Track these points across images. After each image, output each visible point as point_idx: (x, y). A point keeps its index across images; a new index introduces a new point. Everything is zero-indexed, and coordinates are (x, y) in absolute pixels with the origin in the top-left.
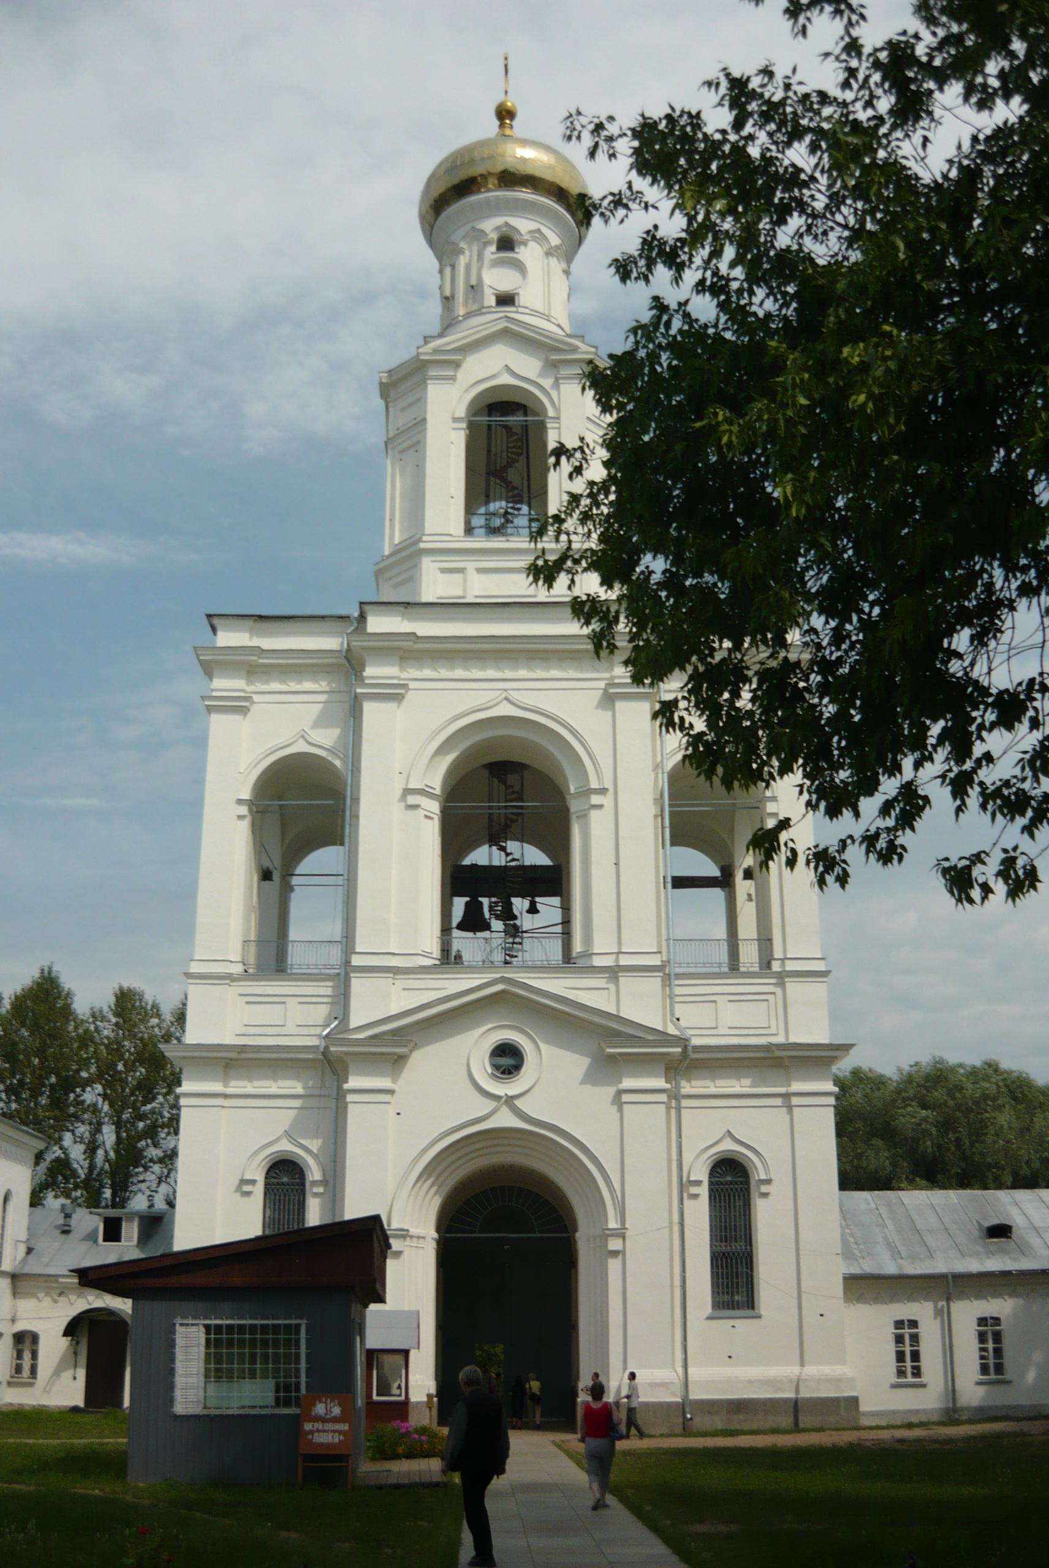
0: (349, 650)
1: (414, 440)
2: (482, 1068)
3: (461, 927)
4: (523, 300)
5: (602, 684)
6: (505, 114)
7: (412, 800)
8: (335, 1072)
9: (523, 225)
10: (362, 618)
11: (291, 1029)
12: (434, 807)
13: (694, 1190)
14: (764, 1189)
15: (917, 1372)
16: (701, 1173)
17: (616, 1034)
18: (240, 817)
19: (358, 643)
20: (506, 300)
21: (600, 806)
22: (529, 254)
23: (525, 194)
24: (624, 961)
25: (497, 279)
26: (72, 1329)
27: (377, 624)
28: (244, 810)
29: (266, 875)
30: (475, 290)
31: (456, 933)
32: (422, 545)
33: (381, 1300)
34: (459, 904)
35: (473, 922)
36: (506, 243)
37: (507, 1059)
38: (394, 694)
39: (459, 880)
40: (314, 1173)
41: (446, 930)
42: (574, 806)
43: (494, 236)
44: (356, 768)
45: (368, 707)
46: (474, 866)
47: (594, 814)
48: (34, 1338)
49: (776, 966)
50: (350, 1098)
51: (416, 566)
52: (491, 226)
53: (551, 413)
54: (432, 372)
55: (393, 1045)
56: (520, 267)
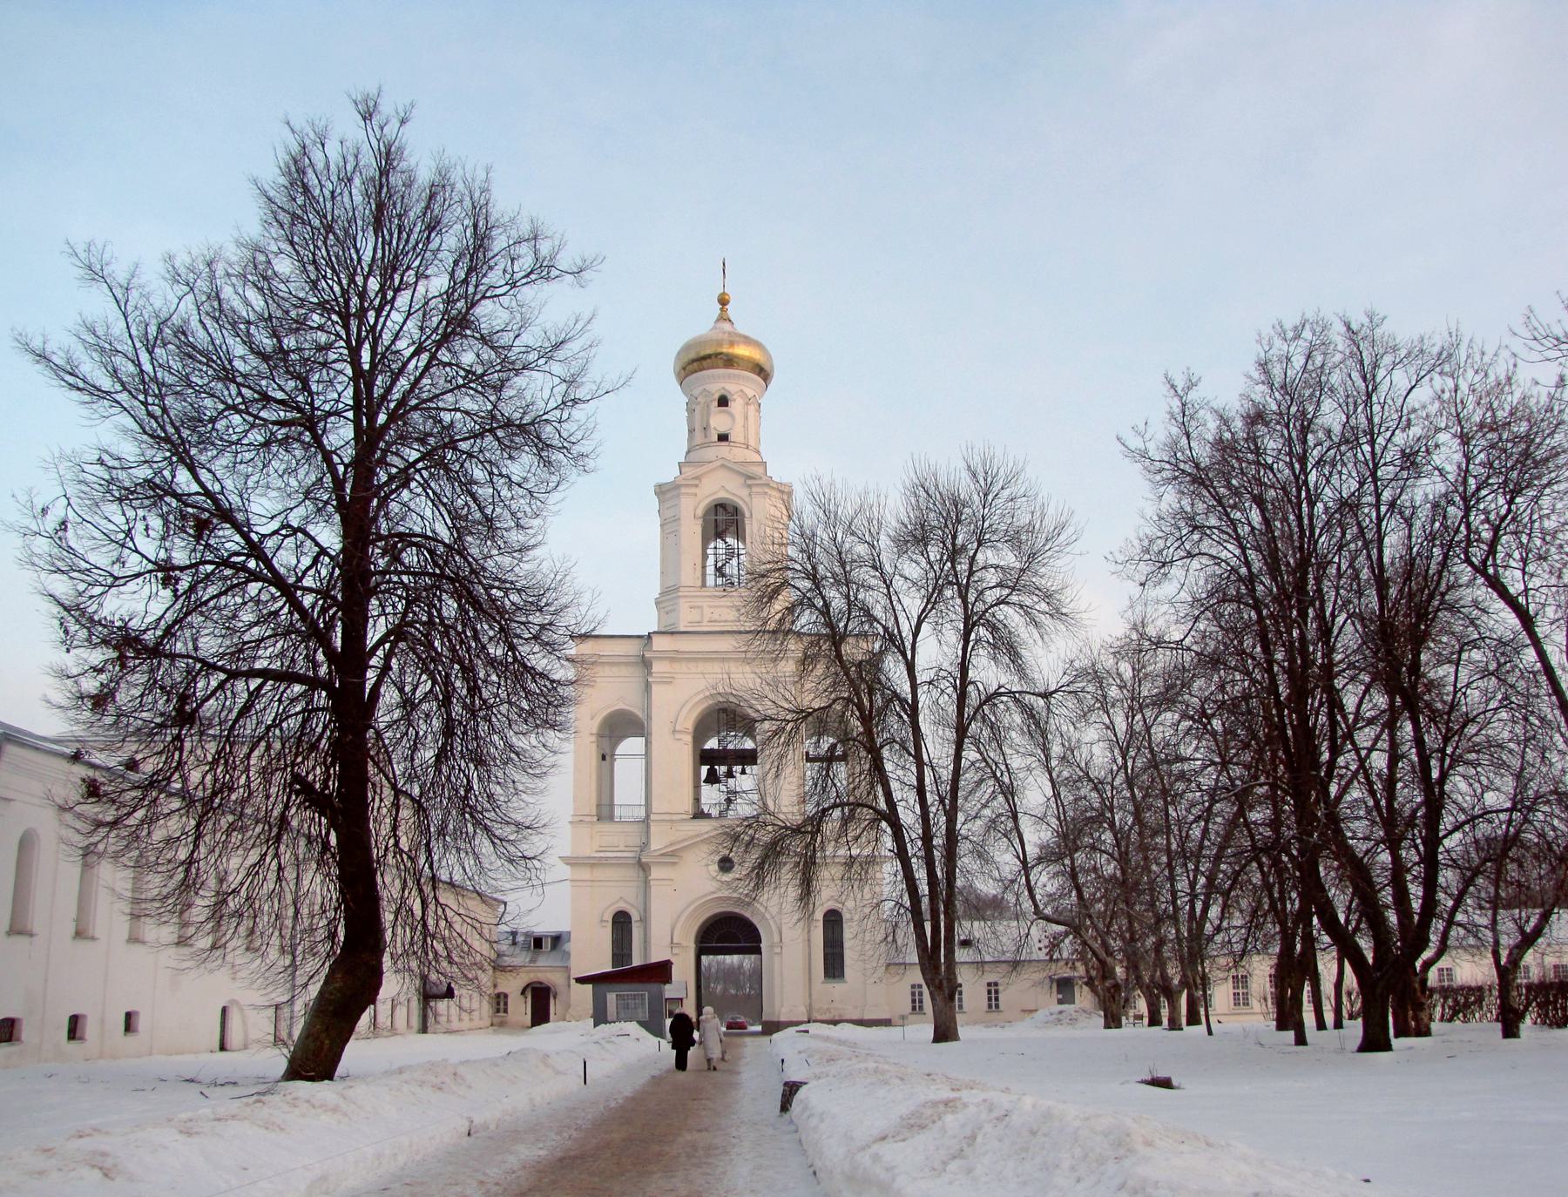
4: (731, 438)
6: (723, 301)
7: (678, 736)
9: (731, 388)
15: (997, 1006)
20: (723, 438)
26: (523, 993)
27: (660, 643)
28: (593, 739)
29: (604, 758)
34: (704, 769)
35: (713, 778)
36: (723, 402)
38: (668, 681)
40: (635, 917)
41: (697, 787)
43: (717, 396)
44: (649, 717)
45: (655, 688)
48: (506, 996)
52: (716, 389)
53: (747, 514)
54: (683, 490)
55: (672, 856)
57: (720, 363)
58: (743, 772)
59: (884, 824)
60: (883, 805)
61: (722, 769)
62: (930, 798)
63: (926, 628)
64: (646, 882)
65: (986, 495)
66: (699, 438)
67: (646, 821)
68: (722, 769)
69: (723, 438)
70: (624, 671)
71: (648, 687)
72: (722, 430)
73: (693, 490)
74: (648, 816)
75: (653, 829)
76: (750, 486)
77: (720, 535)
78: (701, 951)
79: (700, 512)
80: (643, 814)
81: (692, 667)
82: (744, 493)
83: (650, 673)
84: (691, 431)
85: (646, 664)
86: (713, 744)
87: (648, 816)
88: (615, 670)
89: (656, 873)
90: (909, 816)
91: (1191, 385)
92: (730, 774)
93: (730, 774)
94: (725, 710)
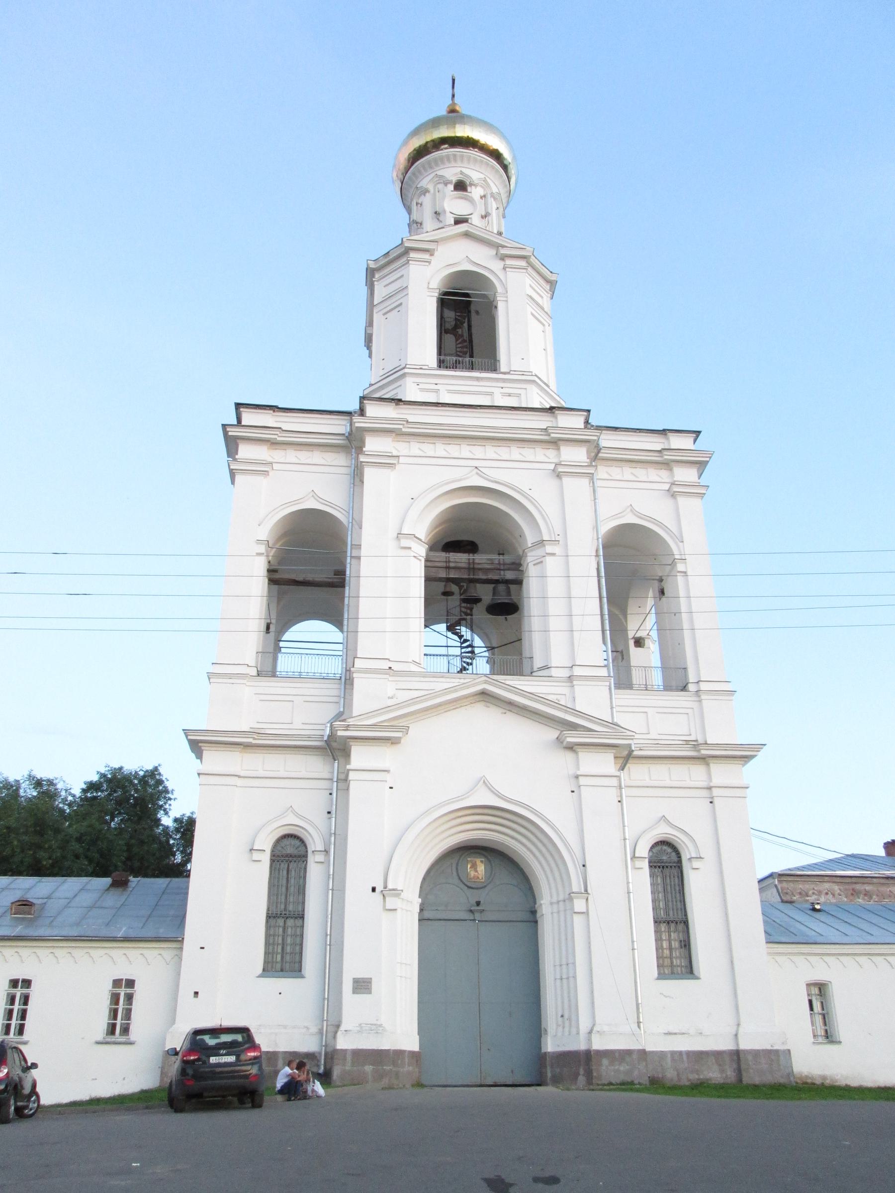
0: (350, 434)
1: (399, 302)
5: (552, 467)
7: (405, 542)
10: (362, 412)
12: (422, 550)
13: (638, 864)
14: (696, 864)
16: (643, 851)
17: (574, 727)
18: (259, 554)
19: (359, 422)
21: (553, 554)
23: (474, 153)
24: (577, 671)
25: (454, 205)
28: (262, 549)
32: (406, 370)
38: (388, 462)
40: (315, 843)
42: (531, 558)
43: (454, 179)
45: (368, 472)
47: (548, 559)
49: (692, 687)
50: (352, 775)
52: (452, 173)
53: (500, 289)
54: (412, 255)
64: (344, 781)
67: (347, 681)
70: (317, 457)
71: (357, 476)
73: (426, 256)
76: (503, 258)
81: (428, 448)
82: (497, 266)
85: (353, 443)
87: (348, 671)
88: (304, 456)
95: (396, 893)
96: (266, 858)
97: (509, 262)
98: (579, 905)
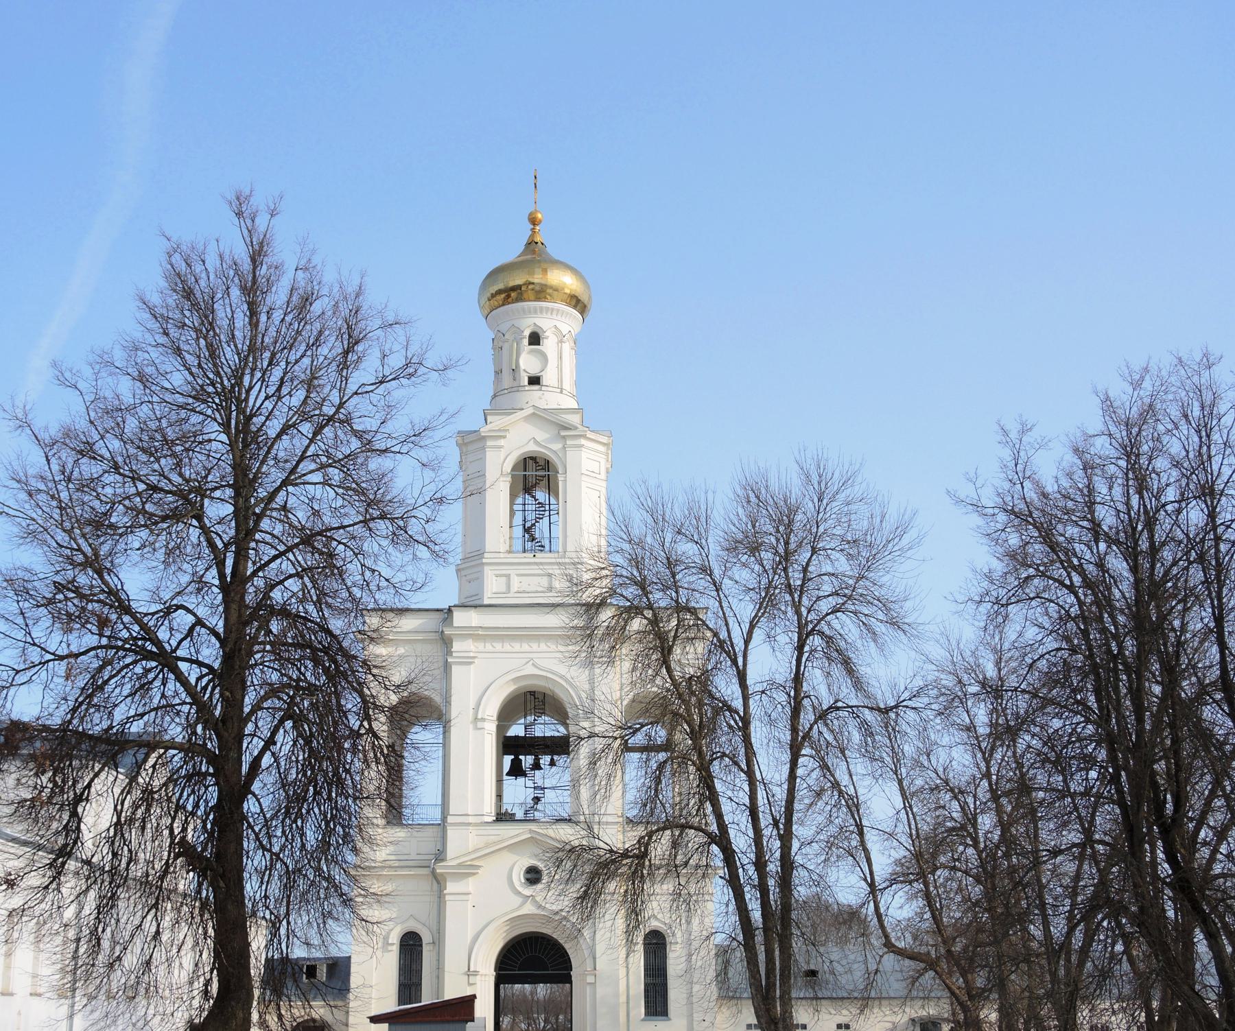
2: (519, 877)
3: (508, 774)
4: (544, 381)
6: (534, 221)
8: (438, 882)
11: (413, 856)
20: (535, 381)
22: (549, 344)
27: (460, 618)
30: (515, 371)
31: (505, 777)
33: (473, 1020)
34: (508, 759)
35: (516, 771)
36: (535, 339)
37: (533, 876)
38: (468, 662)
39: (509, 745)
40: (426, 939)
41: (499, 781)
43: (527, 333)
44: (448, 701)
45: (454, 668)
46: (517, 737)
50: (447, 898)
51: (482, 572)
54: (489, 443)
56: (544, 358)
57: (531, 294)
58: (552, 763)
59: (715, 848)
60: (714, 828)
61: (527, 761)
62: (765, 820)
63: (758, 635)
64: (441, 897)
65: (820, 500)
66: (507, 381)
68: (527, 761)
69: (535, 381)
72: (534, 372)
74: (444, 819)
75: (451, 832)
77: (528, 489)
78: (500, 980)
79: (508, 467)
80: (439, 816)
83: (449, 652)
84: (498, 372)
86: (517, 730)
89: (451, 887)
90: (741, 841)
91: (1024, 431)
92: (536, 766)
93: (536, 766)
94: (532, 693)
95: (476, 973)
96: (395, 949)
97: (569, 442)
98: (590, 979)
